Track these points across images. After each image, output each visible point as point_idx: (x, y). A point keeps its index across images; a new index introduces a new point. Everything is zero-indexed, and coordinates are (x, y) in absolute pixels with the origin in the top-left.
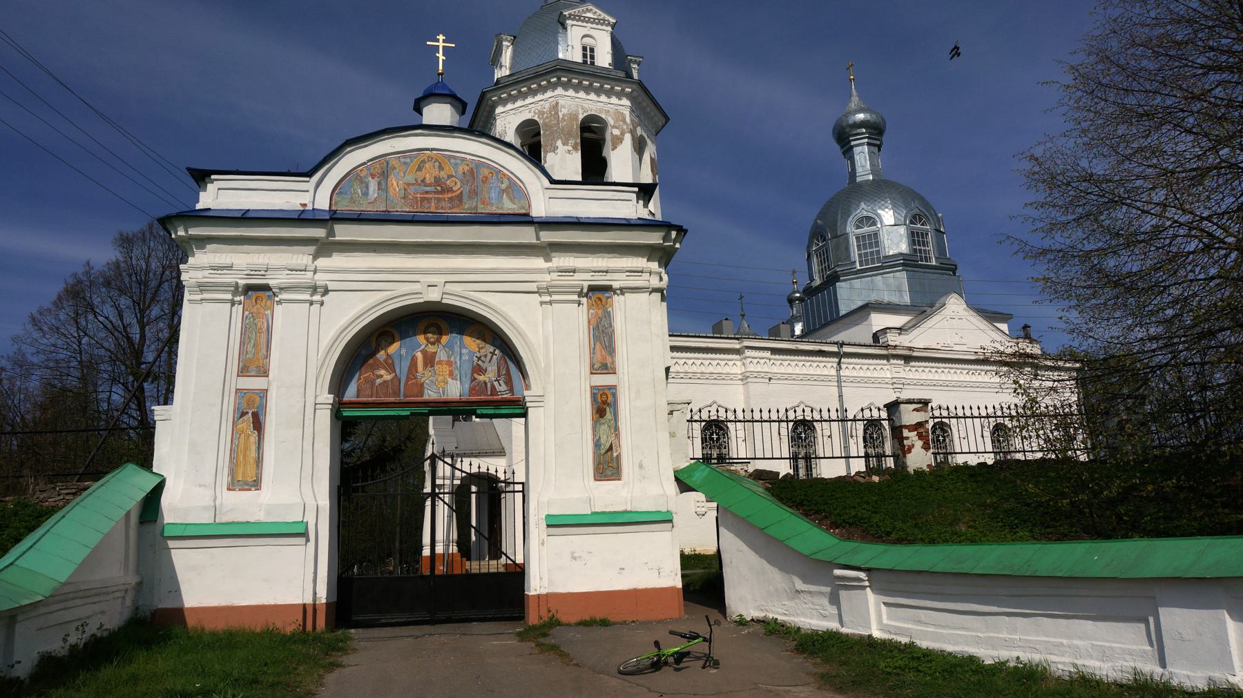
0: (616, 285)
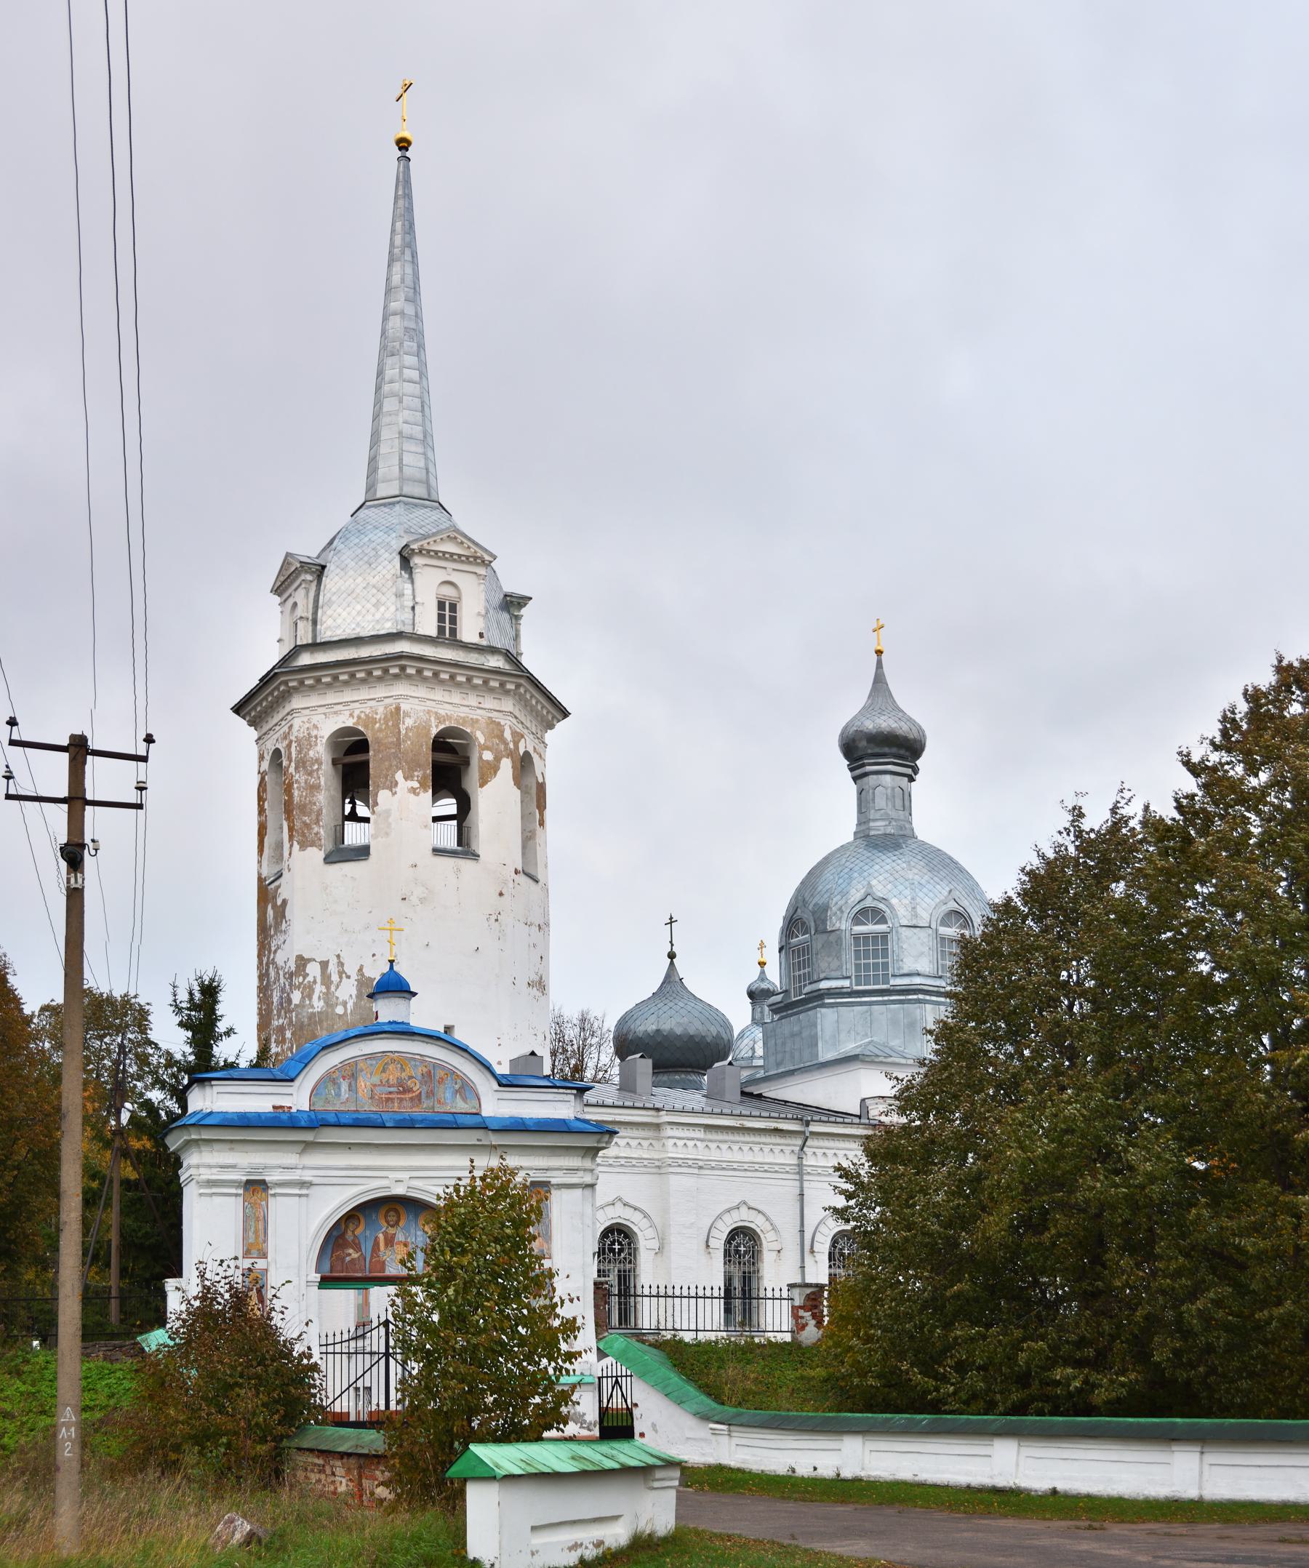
0: (554, 1181)
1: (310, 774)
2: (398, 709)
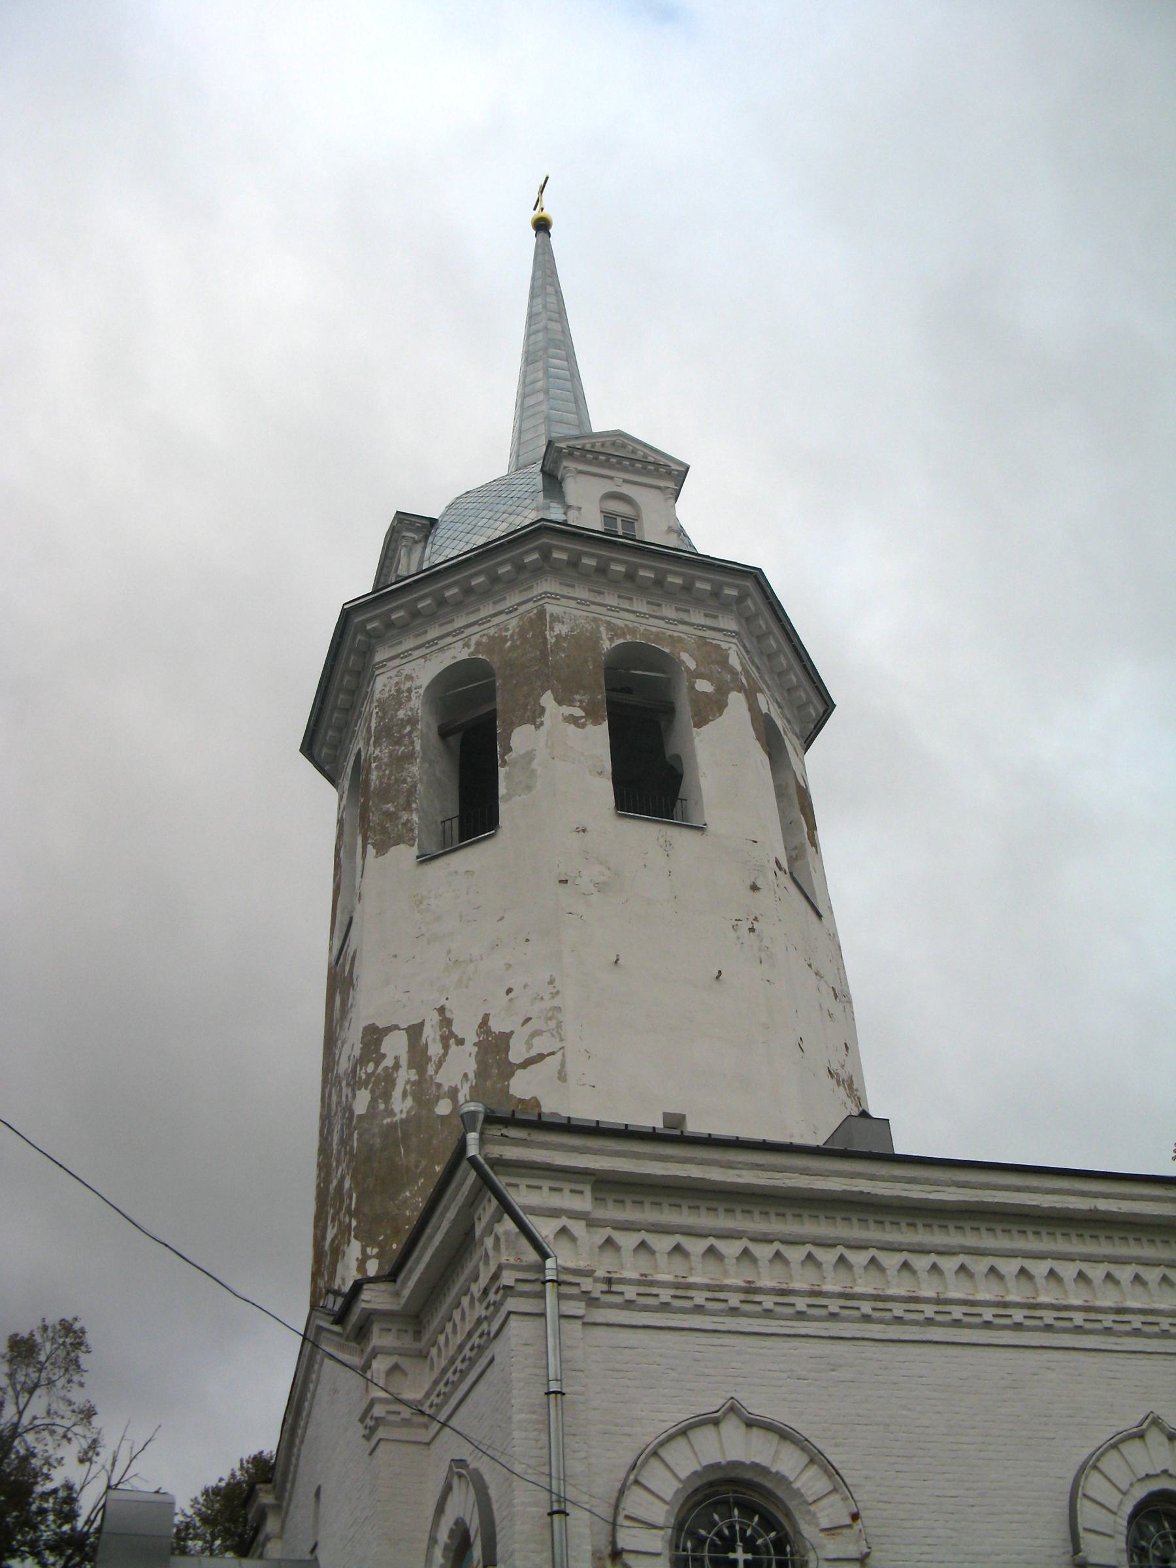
1: (398, 742)
2: (541, 613)
